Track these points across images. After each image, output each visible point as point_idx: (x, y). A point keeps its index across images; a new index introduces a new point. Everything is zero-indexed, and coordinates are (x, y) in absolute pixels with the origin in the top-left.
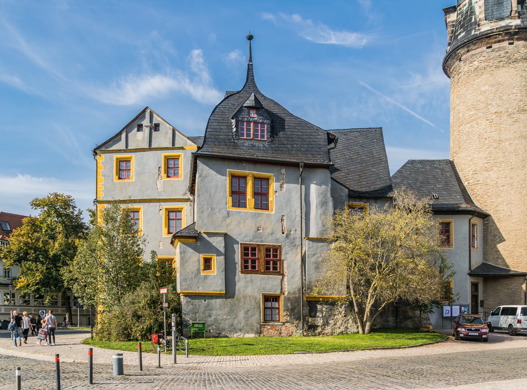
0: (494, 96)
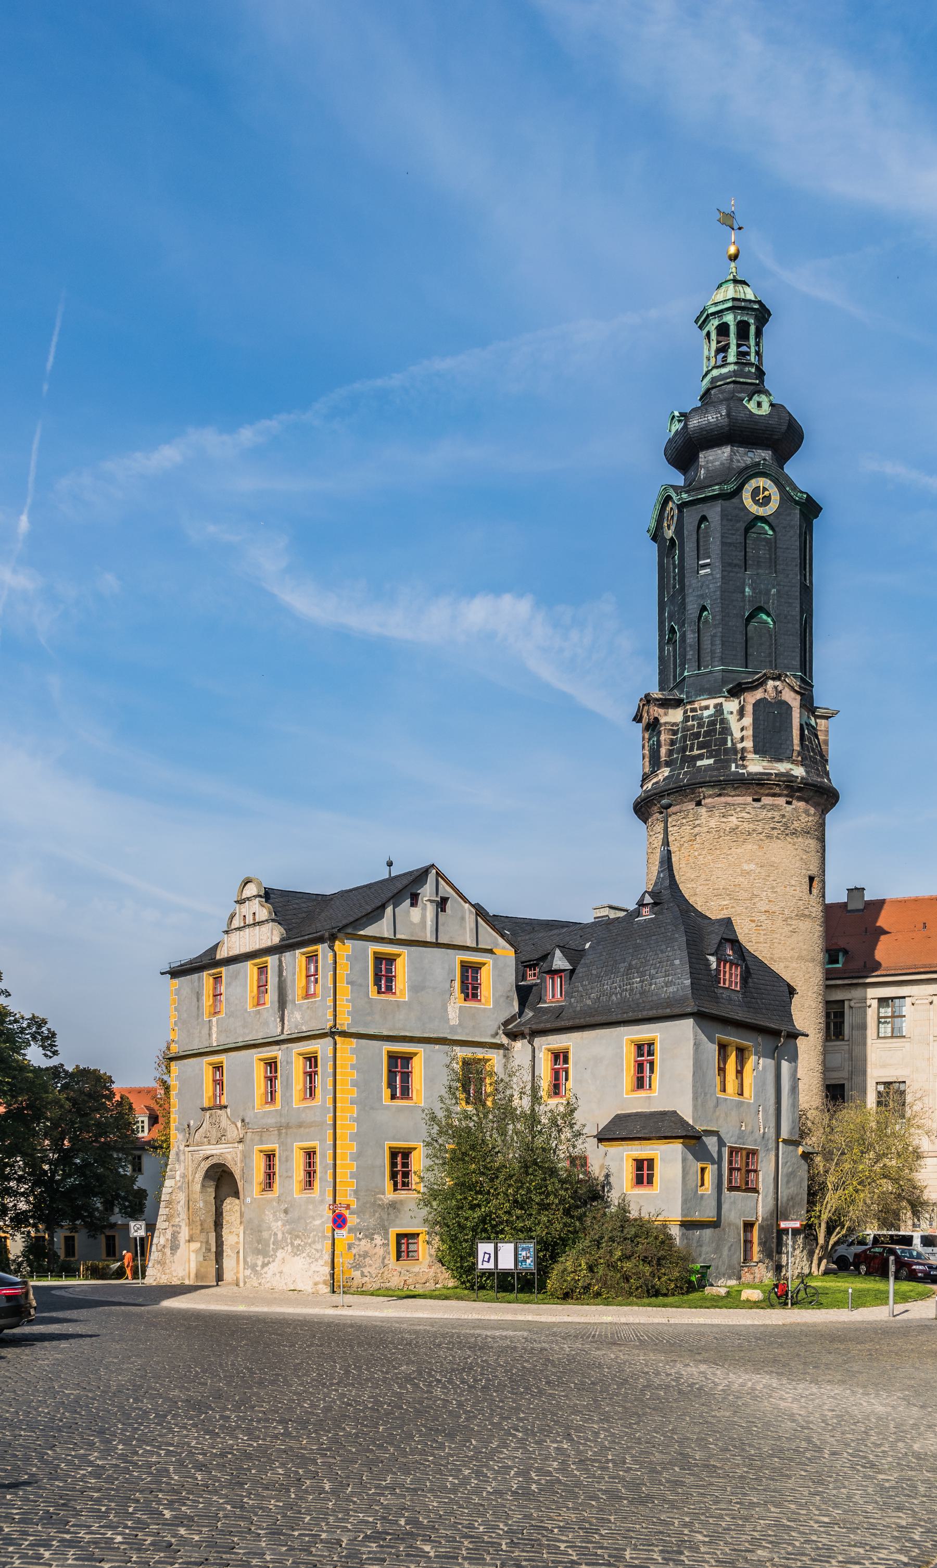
0: (765, 884)
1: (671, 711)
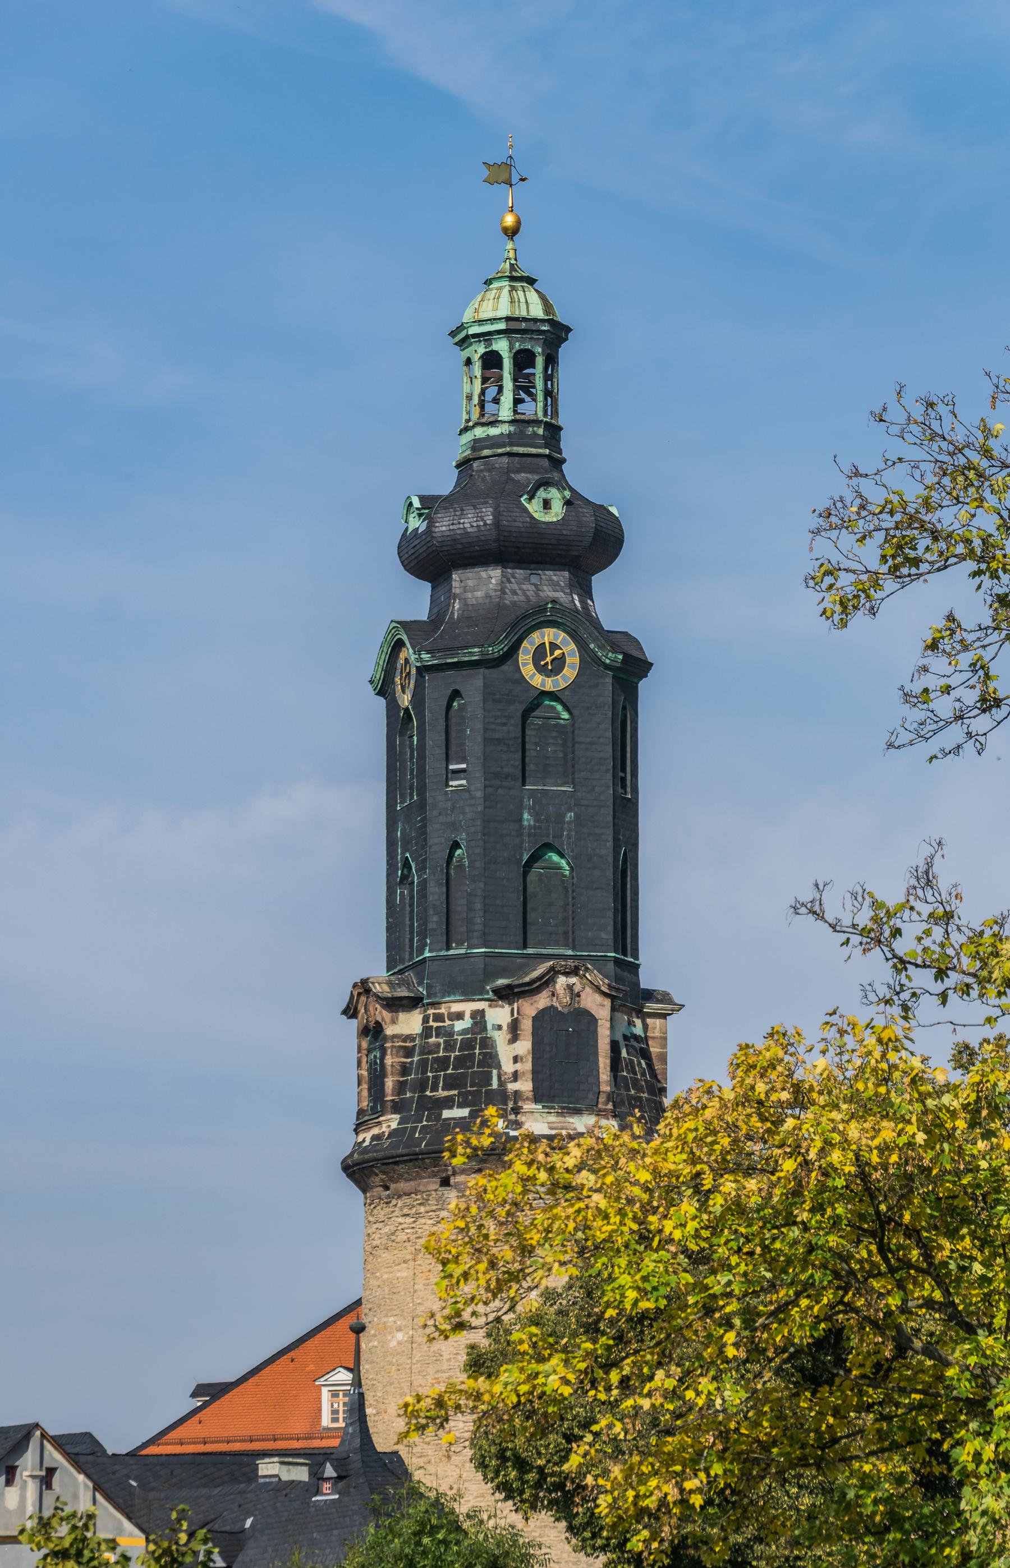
1: (402, 1016)
